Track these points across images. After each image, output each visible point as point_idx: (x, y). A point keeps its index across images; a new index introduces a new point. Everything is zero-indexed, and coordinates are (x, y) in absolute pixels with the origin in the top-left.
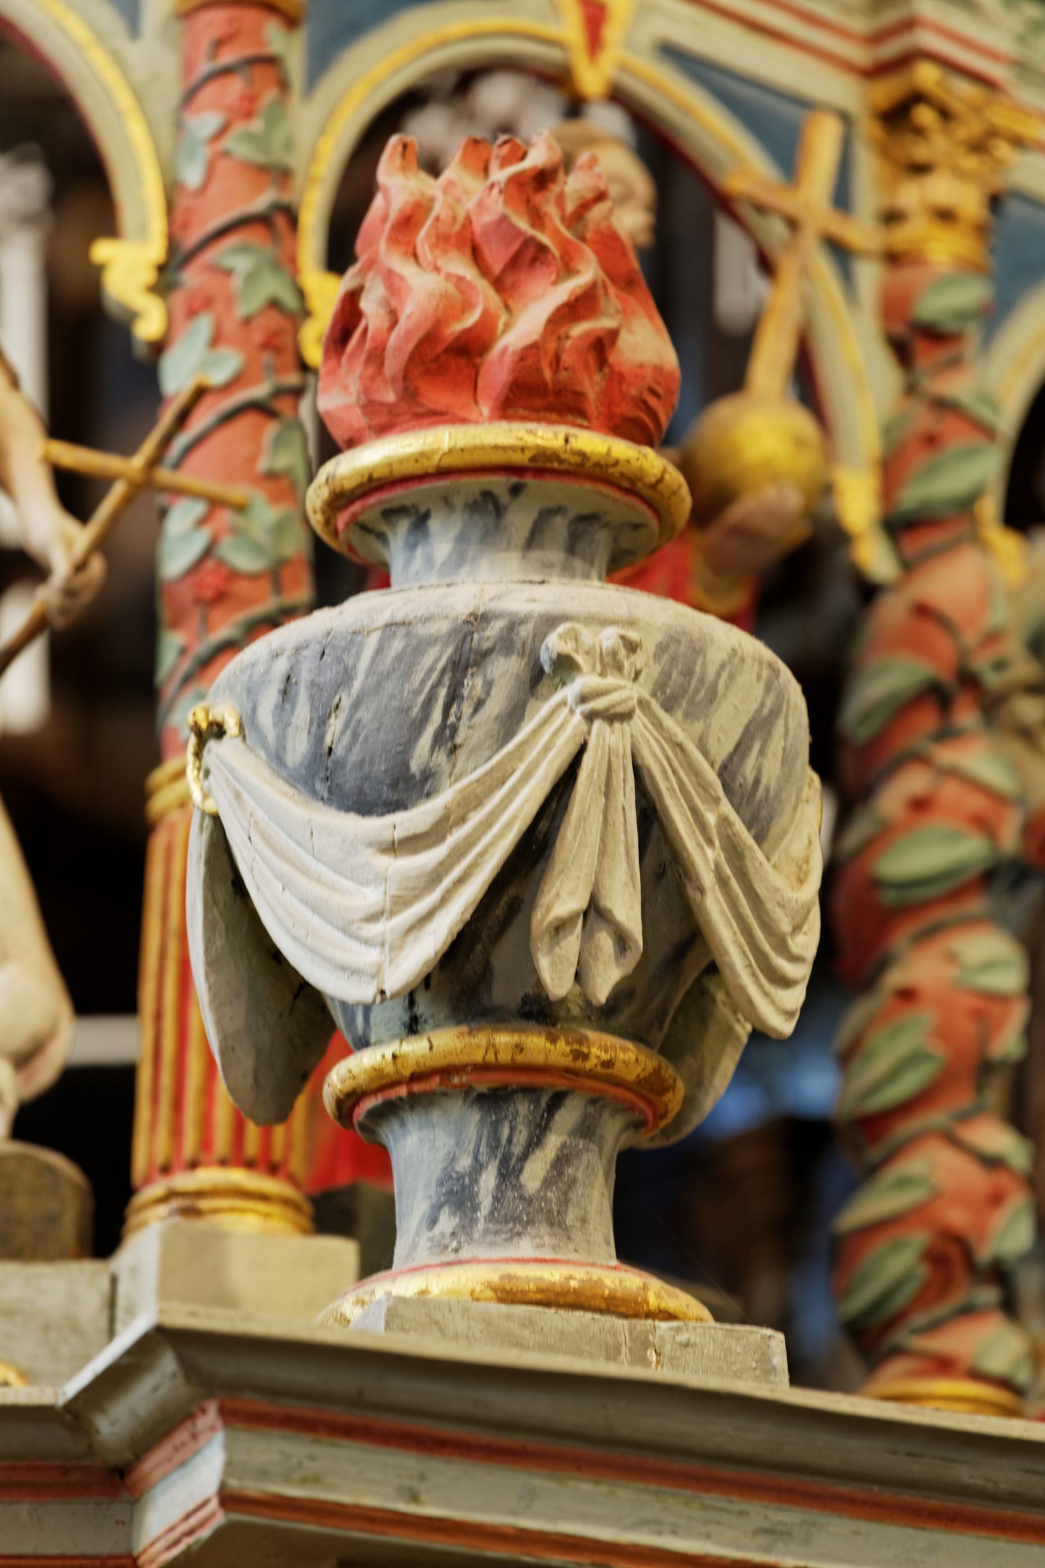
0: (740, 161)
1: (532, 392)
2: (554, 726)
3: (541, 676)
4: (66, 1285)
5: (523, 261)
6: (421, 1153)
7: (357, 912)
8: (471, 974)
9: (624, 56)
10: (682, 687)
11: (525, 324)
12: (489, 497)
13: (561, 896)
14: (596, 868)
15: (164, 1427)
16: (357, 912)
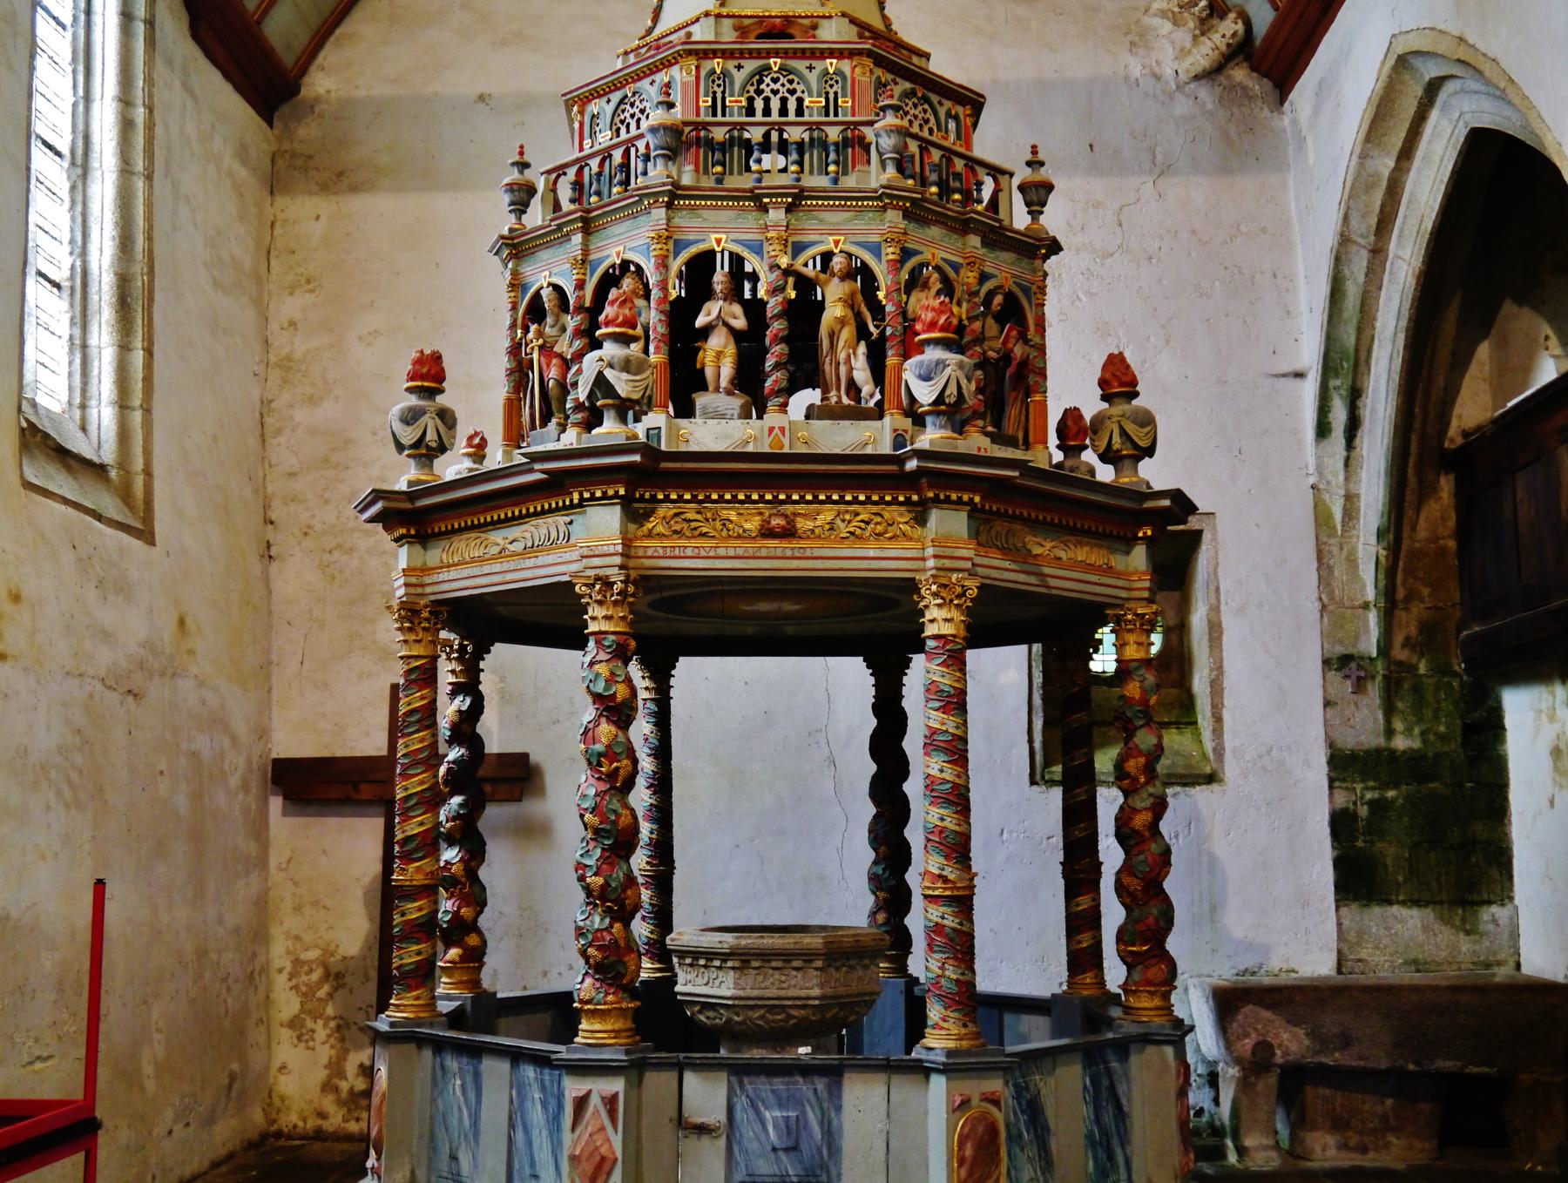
0: (952, 274)
1: (942, 329)
2: (948, 371)
3: (945, 366)
4: (877, 424)
5: (942, 312)
6: (929, 420)
7: (925, 394)
8: (939, 400)
9: (938, 261)
10: (961, 366)
11: (942, 320)
12: (936, 342)
13: (948, 392)
14: (952, 389)
15: (910, 458)
16: (925, 394)
